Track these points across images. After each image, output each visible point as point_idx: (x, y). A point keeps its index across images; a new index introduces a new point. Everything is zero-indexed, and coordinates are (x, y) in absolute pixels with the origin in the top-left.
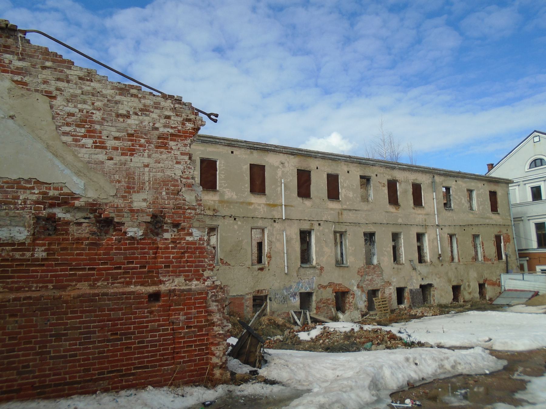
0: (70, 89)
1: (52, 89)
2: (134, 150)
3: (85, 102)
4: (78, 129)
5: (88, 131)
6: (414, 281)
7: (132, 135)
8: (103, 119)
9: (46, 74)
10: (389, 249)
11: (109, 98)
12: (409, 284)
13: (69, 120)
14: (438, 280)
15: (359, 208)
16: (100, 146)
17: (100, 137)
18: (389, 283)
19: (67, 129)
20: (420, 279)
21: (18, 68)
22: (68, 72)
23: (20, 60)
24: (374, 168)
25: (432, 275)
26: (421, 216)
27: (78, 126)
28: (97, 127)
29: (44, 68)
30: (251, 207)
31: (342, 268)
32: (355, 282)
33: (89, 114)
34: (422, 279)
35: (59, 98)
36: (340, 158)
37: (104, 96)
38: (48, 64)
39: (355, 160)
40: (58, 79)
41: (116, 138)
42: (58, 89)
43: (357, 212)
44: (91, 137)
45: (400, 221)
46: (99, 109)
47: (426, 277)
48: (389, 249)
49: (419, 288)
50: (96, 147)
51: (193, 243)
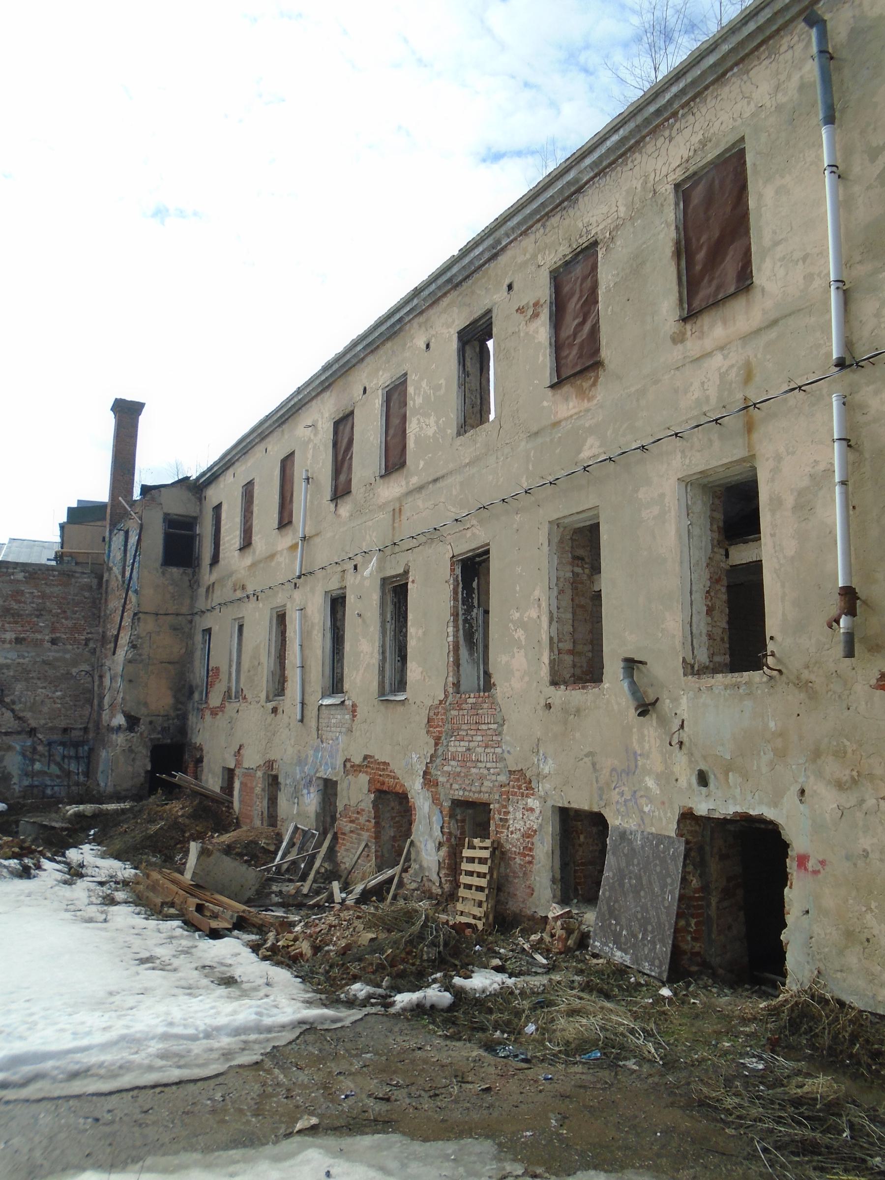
6: (650, 782)
10: (533, 613)
12: (615, 796)
14: (828, 800)
15: (451, 466)
18: (523, 782)
20: (686, 777)
24: (503, 259)
25: (781, 754)
26: (718, 360)
30: (273, 564)
31: (391, 705)
32: (417, 761)
34: (703, 779)
36: (397, 317)
39: (433, 286)
43: (438, 485)
45: (591, 449)
47: (728, 769)
48: (533, 613)
49: (671, 829)
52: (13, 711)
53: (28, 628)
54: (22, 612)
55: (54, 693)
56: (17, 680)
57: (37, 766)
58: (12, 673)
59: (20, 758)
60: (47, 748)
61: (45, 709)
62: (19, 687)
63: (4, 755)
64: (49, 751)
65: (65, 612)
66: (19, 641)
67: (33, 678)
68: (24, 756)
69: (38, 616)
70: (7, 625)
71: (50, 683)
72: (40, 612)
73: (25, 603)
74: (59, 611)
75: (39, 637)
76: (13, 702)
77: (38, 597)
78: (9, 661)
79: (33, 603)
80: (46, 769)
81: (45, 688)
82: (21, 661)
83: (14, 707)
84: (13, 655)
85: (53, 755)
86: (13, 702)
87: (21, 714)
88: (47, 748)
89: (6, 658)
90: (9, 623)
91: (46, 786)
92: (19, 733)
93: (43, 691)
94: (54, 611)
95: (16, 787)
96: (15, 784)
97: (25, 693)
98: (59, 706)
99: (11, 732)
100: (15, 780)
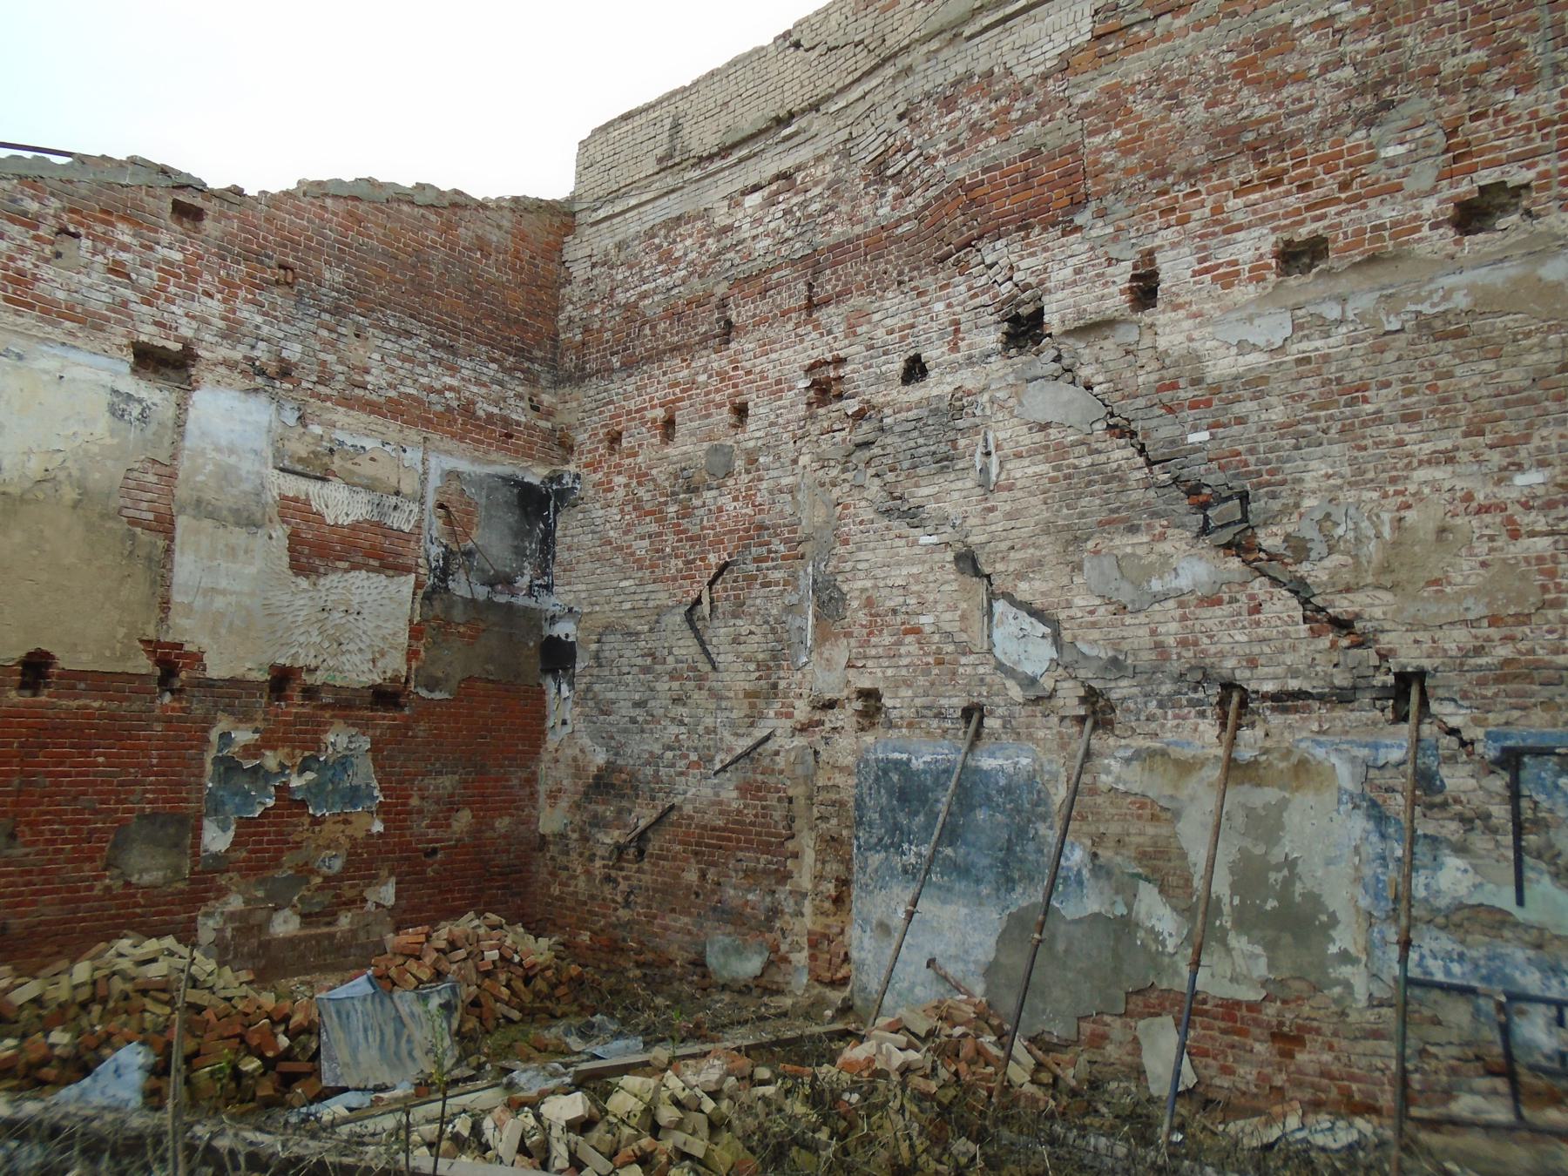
52: (1300, 590)
53: (1330, 185)
54: (1290, 126)
55: (1502, 477)
56: (1303, 440)
57: (1451, 879)
58: (1277, 414)
59: (1359, 824)
60: (1498, 783)
61: (1465, 572)
62: (1317, 470)
63: (1283, 805)
64: (1515, 796)
65: (1511, 52)
66: (1297, 256)
67: (1378, 418)
68: (1378, 815)
69: (1367, 121)
70: (1233, 203)
71: (1475, 431)
72: (1376, 100)
73: (1299, 77)
74: (1478, 55)
75: (1388, 213)
76: (1299, 548)
77: (1359, 27)
78: (1256, 359)
79: (1339, 63)
80: (1505, 898)
81: (1449, 458)
82: (1315, 345)
83: (1303, 569)
84: (1273, 328)
85: (1540, 825)
86: (1299, 548)
87: (1342, 606)
88: (1498, 783)
89: (1243, 347)
90: (1245, 188)
91: (1518, 998)
92: (1343, 697)
93: (1440, 473)
94: (1449, 66)
95: (1357, 977)
96: (1345, 957)
97: (1349, 496)
98: (1543, 544)
99: (1300, 695)
100: (1345, 938)
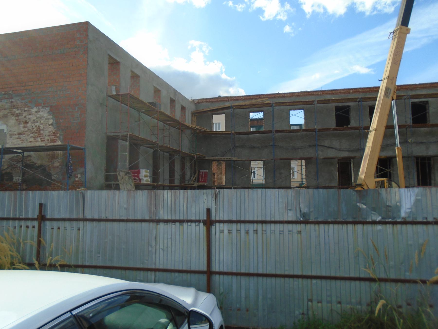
0: (33, 118)
1: (27, 119)
2: (55, 140)
3: (37, 122)
4: (35, 134)
5: (39, 135)
7: (54, 133)
8: (44, 128)
9: (25, 114)
11: (46, 118)
13: (32, 131)
16: (43, 141)
17: (43, 136)
19: (32, 135)
21: (17, 114)
22: (32, 110)
23: (18, 110)
27: (36, 133)
28: (42, 132)
29: (25, 111)
33: (39, 127)
35: (30, 123)
37: (44, 117)
38: (26, 109)
40: (30, 115)
41: (49, 136)
42: (29, 119)
44: (40, 137)
46: (42, 124)
50: (42, 141)
51: (78, 181)
